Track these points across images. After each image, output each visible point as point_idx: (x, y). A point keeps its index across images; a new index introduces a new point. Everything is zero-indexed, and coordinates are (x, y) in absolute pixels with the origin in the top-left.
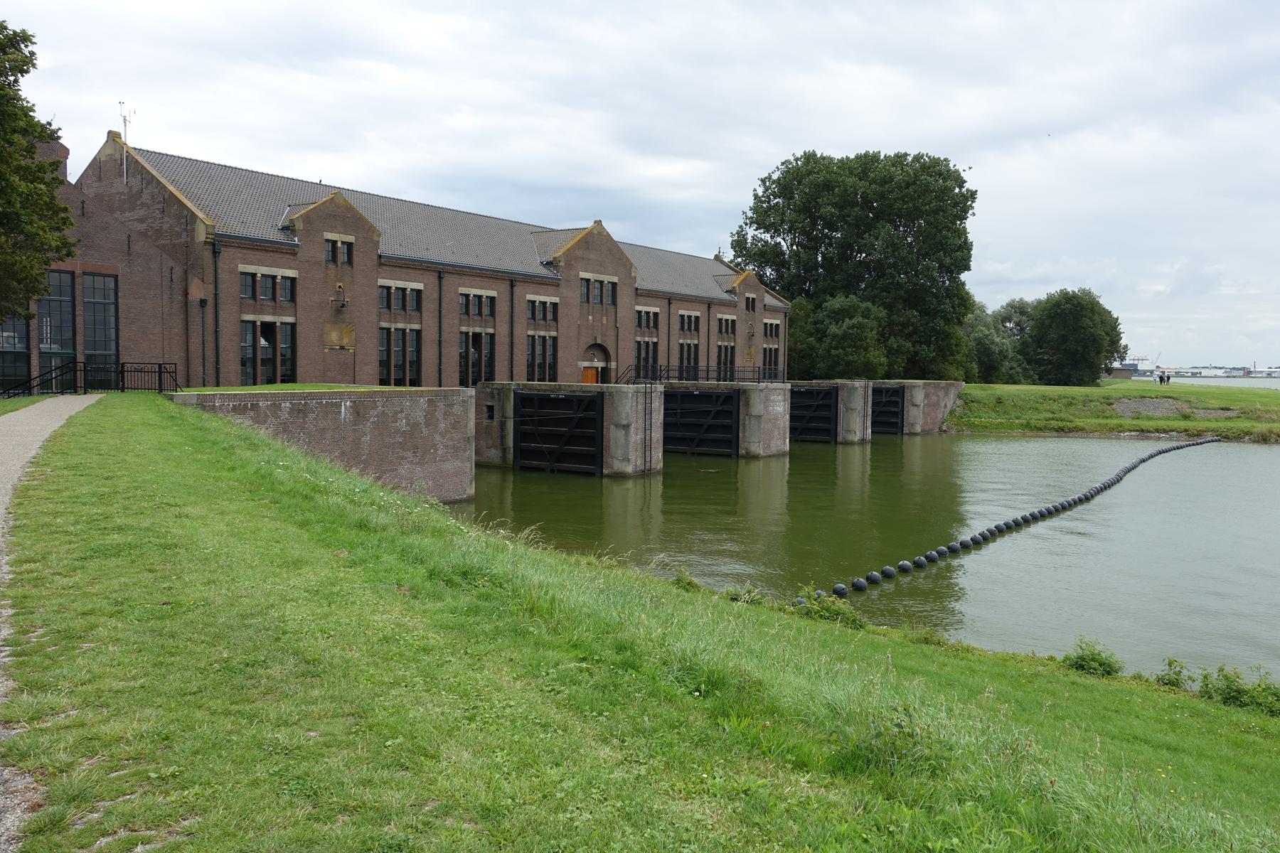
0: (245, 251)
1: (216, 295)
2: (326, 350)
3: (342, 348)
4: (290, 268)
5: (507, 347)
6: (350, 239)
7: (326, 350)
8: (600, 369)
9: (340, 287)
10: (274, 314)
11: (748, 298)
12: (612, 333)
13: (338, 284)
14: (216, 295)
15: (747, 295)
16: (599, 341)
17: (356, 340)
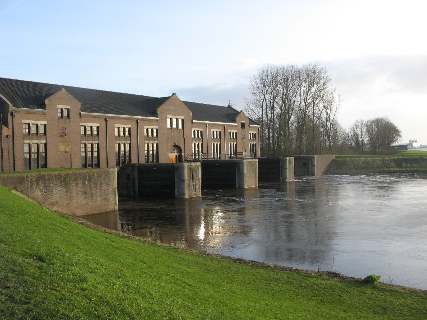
0: (25, 115)
1: (13, 133)
2: (59, 153)
3: (66, 152)
4: (43, 120)
5: (136, 149)
6: (68, 107)
7: (59, 153)
8: (177, 156)
9: (64, 127)
10: (37, 140)
11: (242, 123)
12: (182, 140)
13: (63, 126)
14: (13, 133)
15: (241, 122)
16: (176, 144)
17: (72, 149)
